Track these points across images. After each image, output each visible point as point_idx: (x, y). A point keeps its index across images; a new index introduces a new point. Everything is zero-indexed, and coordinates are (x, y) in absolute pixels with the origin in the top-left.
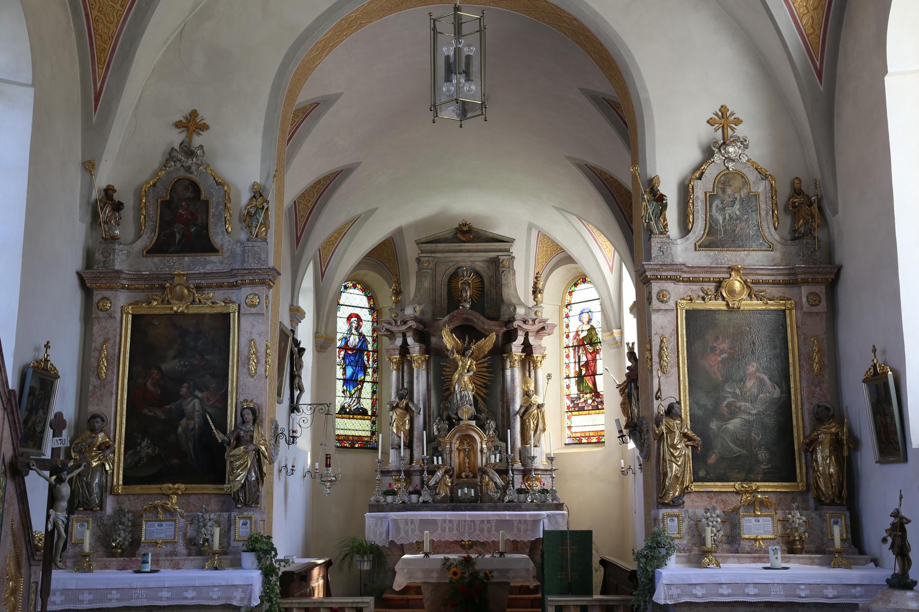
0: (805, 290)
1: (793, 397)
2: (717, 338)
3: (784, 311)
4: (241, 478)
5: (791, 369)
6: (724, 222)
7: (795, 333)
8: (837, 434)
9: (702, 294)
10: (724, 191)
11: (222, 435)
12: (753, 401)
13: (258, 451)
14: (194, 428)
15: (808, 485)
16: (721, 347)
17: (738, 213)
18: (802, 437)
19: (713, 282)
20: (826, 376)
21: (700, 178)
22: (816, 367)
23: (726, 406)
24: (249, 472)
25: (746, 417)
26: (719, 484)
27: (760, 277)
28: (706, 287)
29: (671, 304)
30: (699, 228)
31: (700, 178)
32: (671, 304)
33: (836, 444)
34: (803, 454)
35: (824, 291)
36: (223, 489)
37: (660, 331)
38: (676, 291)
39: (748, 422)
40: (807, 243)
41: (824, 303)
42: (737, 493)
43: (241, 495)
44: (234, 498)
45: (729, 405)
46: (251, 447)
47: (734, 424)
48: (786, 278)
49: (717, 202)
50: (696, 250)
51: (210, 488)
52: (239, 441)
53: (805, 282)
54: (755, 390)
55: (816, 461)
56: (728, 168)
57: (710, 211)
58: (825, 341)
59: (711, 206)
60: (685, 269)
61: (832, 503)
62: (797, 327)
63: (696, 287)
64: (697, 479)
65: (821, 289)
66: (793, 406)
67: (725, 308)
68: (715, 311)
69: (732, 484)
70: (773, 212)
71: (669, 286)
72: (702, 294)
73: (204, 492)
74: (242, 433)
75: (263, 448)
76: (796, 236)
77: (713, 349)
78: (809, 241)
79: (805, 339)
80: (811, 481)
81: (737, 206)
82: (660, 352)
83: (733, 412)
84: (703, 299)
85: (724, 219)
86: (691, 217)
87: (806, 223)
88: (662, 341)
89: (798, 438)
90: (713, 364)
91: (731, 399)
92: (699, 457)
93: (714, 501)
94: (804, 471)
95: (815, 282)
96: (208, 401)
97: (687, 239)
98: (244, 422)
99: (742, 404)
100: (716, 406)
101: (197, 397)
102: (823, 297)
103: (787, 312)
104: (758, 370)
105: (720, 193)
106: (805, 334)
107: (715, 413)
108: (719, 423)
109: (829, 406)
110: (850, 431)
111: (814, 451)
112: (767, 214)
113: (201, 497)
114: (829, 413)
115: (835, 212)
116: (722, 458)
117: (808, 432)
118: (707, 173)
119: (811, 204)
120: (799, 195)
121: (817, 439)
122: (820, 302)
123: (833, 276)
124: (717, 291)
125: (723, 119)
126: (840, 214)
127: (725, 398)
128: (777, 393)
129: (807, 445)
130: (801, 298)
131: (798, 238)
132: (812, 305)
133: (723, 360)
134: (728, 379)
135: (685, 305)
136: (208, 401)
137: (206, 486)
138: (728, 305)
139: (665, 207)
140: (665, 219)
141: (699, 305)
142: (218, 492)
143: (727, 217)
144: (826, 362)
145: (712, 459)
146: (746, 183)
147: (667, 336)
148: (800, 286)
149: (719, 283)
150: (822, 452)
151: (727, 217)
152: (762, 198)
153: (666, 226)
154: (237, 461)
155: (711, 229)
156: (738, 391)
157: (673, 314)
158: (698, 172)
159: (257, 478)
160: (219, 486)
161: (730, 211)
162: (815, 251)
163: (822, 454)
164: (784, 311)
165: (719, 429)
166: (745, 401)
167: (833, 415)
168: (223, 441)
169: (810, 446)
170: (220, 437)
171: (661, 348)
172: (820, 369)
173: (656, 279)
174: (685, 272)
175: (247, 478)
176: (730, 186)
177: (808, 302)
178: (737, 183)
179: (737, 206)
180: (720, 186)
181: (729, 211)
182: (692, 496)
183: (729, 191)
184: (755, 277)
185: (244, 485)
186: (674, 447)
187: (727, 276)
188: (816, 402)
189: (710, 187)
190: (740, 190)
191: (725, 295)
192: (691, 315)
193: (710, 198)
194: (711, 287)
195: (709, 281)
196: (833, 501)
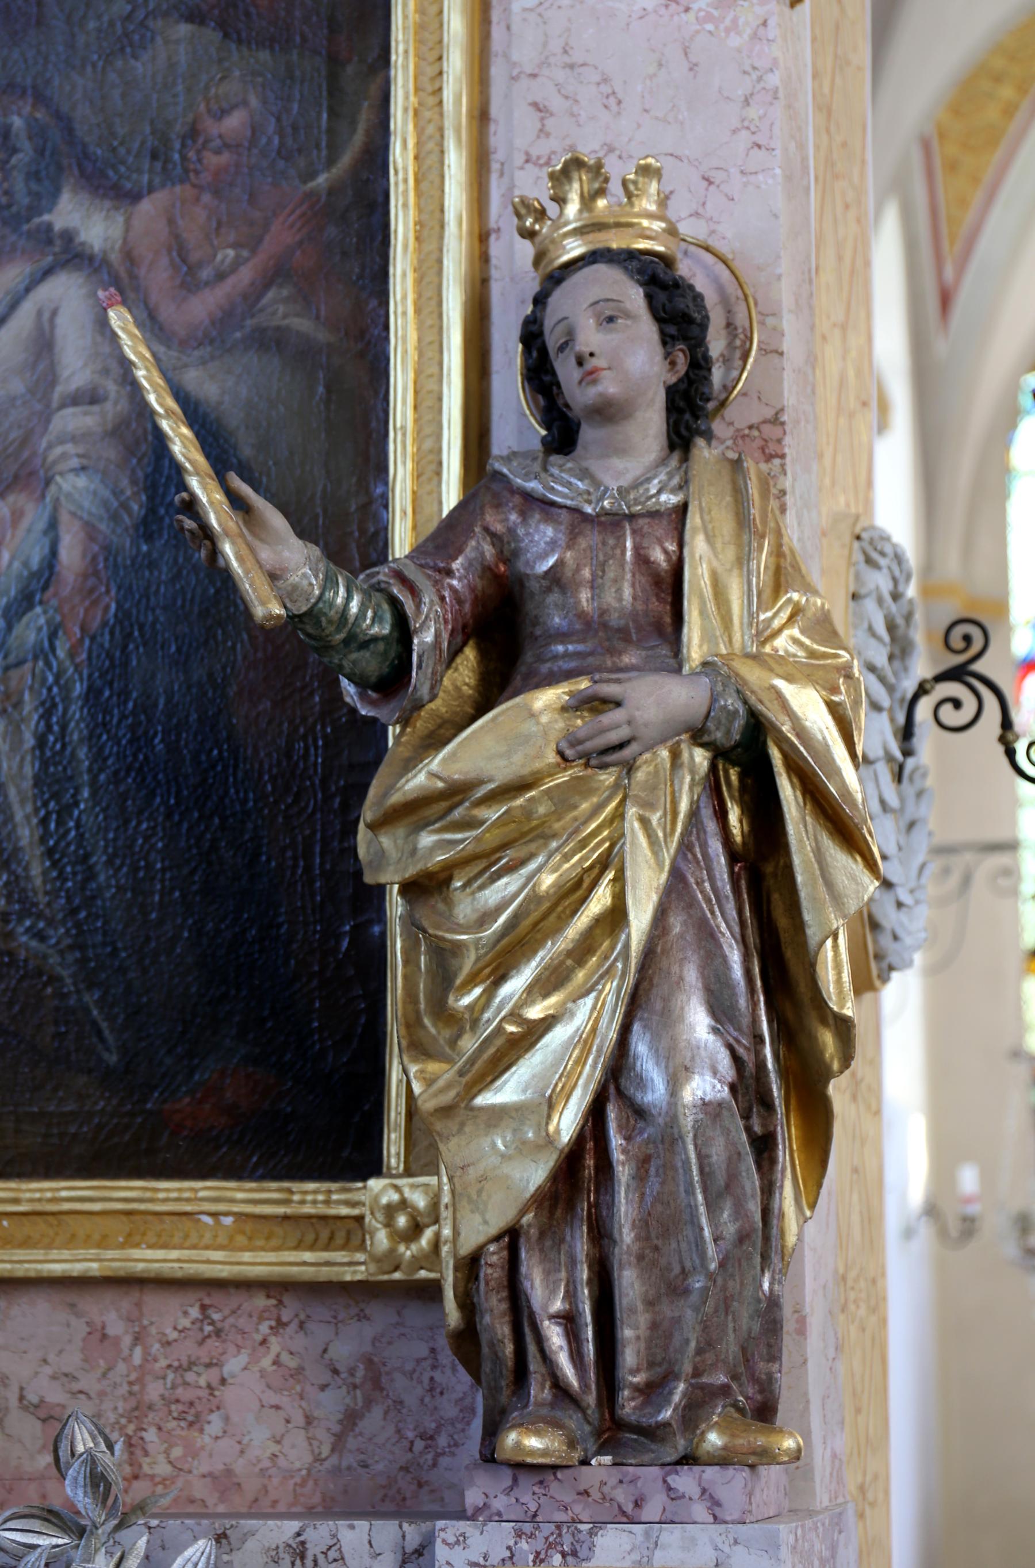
4: (546, 1088)
11: (300, 561)
13: (748, 756)
14: (47, 572)
24: (643, 999)
36: (350, 1231)
43: (546, 1296)
44: (467, 1341)
46: (656, 699)
51: (213, 1222)
52: (504, 636)
73: (146, 1259)
74: (543, 548)
75: (808, 707)
96: (189, 279)
98: (562, 433)
101: (70, 255)
113: (111, 1314)
136: (189, 279)
137: (168, 1192)
142: (303, 1262)
154: (487, 862)
159: (748, 1087)
160: (312, 1196)
168: (306, 634)
170: (271, 567)
175: (619, 1067)
185: (579, 1175)
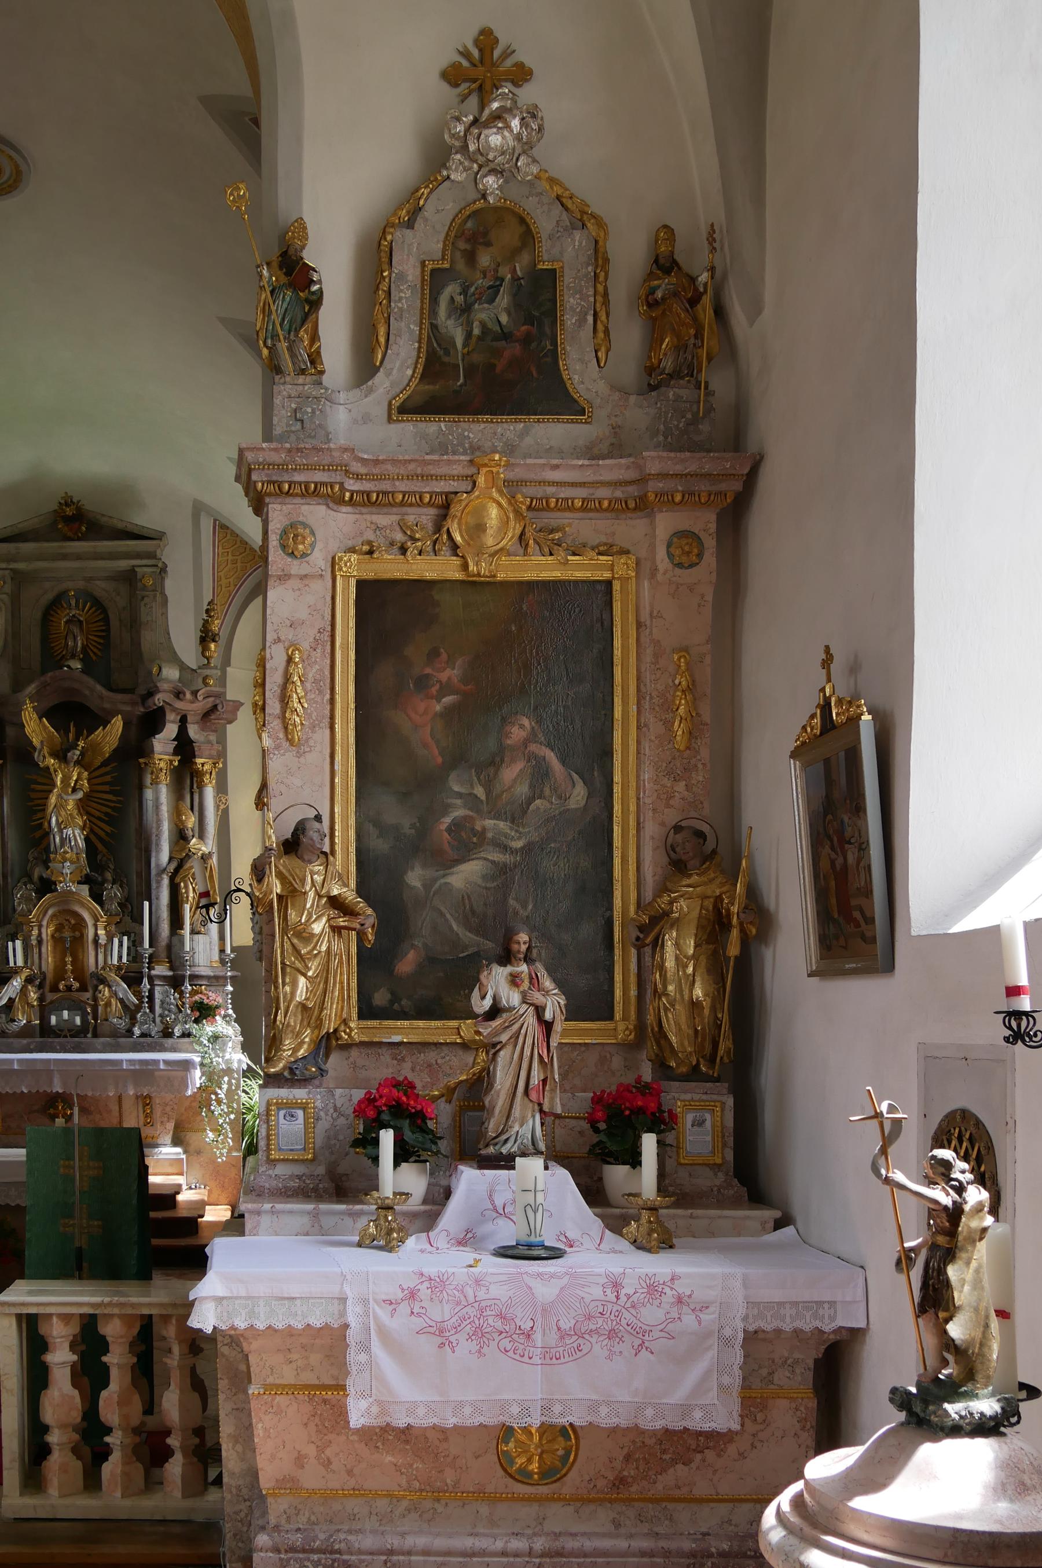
0: (665, 523)
1: (617, 808)
2: (433, 654)
3: (609, 583)
5: (617, 735)
6: (465, 345)
7: (632, 641)
8: (719, 899)
9: (399, 537)
10: (471, 258)
12: (517, 815)
15: (641, 1027)
16: (444, 676)
17: (504, 319)
18: (632, 909)
19: (430, 504)
20: (705, 753)
21: (410, 225)
22: (679, 729)
23: (449, 830)
25: (497, 856)
26: (421, 1023)
27: (550, 490)
28: (411, 519)
29: (319, 559)
30: (401, 365)
31: (410, 225)
32: (319, 559)
33: (715, 927)
34: (633, 952)
35: (713, 527)
37: (288, 634)
38: (331, 527)
39: (502, 870)
40: (678, 398)
41: (710, 558)
42: (465, 1046)
45: (456, 827)
47: (467, 875)
48: (618, 494)
49: (451, 290)
50: (390, 419)
53: (666, 500)
54: (523, 790)
55: (662, 967)
56: (484, 196)
57: (433, 312)
58: (708, 660)
59: (434, 301)
60: (356, 467)
61: (694, 1075)
62: (639, 625)
63: (385, 519)
64: (367, 1011)
65: (704, 522)
66: (617, 830)
67: (459, 576)
68: (431, 583)
69: (454, 1023)
70: (595, 315)
71: (314, 513)
72: (399, 537)
76: (653, 380)
77: (422, 683)
78: (684, 393)
79: (656, 656)
80: (650, 1018)
81: (503, 300)
82: (284, 688)
83: (467, 842)
84: (403, 550)
85: (469, 335)
86: (382, 331)
87: (680, 347)
88: (290, 660)
89: (623, 901)
90: (421, 721)
91: (460, 813)
92: (373, 962)
93: (407, 1066)
94: (633, 992)
95: (690, 500)
97: (371, 391)
99: (489, 823)
100: (424, 829)
102: (710, 543)
103: (616, 586)
104: (532, 737)
105: (461, 266)
106: (657, 643)
107: (418, 846)
108: (430, 873)
109: (705, 828)
110: (753, 893)
111: (657, 944)
112: (582, 321)
114: (706, 847)
115: (755, 310)
116: (431, 960)
117: (648, 895)
118: (429, 212)
119: (694, 301)
120: (667, 271)
121: (666, 914)
122: (700, 555)
123: (738, 486)
124: (438, 529)
125: (483, 72)
126: (767, 312)
127: (446, 809)
128: (578, 795)
129: (642, 928)
130: (652, 547)
131: (652, 388)
132: (680, 565)
133: (449, 713)
134: (457, 759)
135: (354, 567)
138: (465, 567)
139: (315, 302)
140: (315, 337)
141: (391, 567)
143: (476, 331)
144: (707, 717)
145: (407, 964)
146: (528, 236)
147: (305, 645)
148: (651, 516)
149: (445, 506)
150: (677, 945)
151: (476, 331)
152: (568, 279)
153: (315, 358)
155: (434, 363)
156: (480, 791)
157: (320, 588)
158: (408, 211)
161: (483, 316)
162: (695, 421)
163: (679, 949)
164: (609, 583)
165: (427, 885)
166: (497, 817)
167: (714, 852)
169: (650, 930)
171: (287, 679)
172: (691, 734)
173: (281, 493)
174: (358, 477)
176: (488, 244)
177: (670, 555)
178: (507, 236)
179: (503, 300)
180: (462, 245)
181: (482, 314)
182: (354, 1053)
183: (485, 260)
184: (538, 491)
186: (304, 935)
187: (466, 486)
188: (672, 817)
189: (435, 246)
190: (514, 253)
191: (458, 538)
192: (372, 595)
193: (435, 280)
194: (426, 516)
195: (420, 504)
196: (696, 1068)
